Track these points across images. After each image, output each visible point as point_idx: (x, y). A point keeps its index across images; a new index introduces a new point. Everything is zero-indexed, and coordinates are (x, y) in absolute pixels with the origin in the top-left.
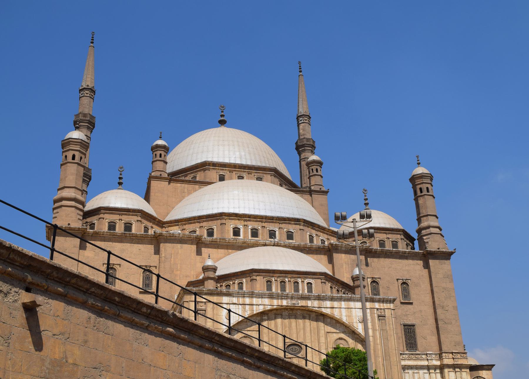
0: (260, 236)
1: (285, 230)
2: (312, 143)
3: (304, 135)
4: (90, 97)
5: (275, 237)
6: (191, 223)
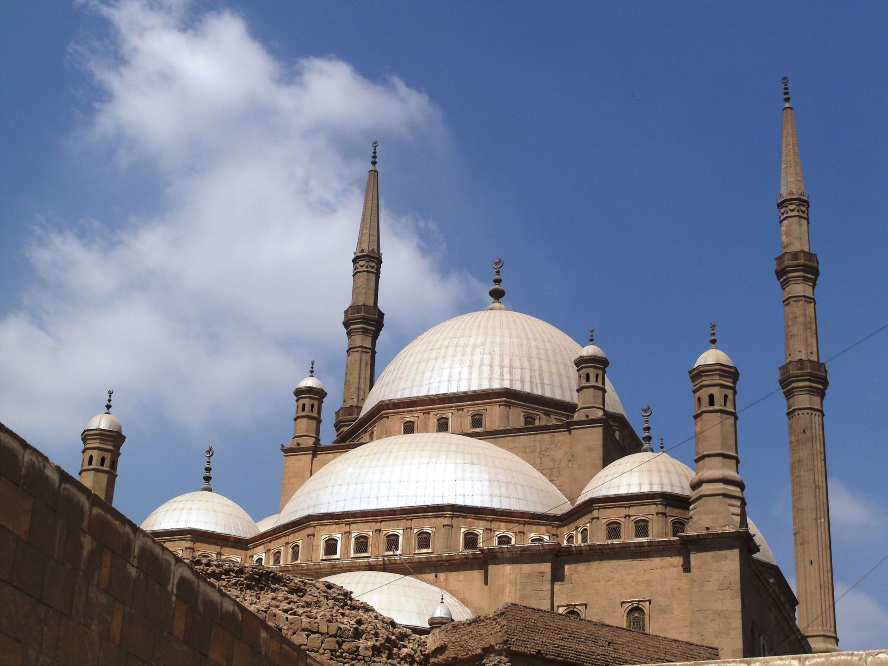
0: (370, 549)
1: (416, 530)
2: (802, 261)
3: (788, 245)
4: (368, 272)
5: (397, 549)
6: (276, 539)
